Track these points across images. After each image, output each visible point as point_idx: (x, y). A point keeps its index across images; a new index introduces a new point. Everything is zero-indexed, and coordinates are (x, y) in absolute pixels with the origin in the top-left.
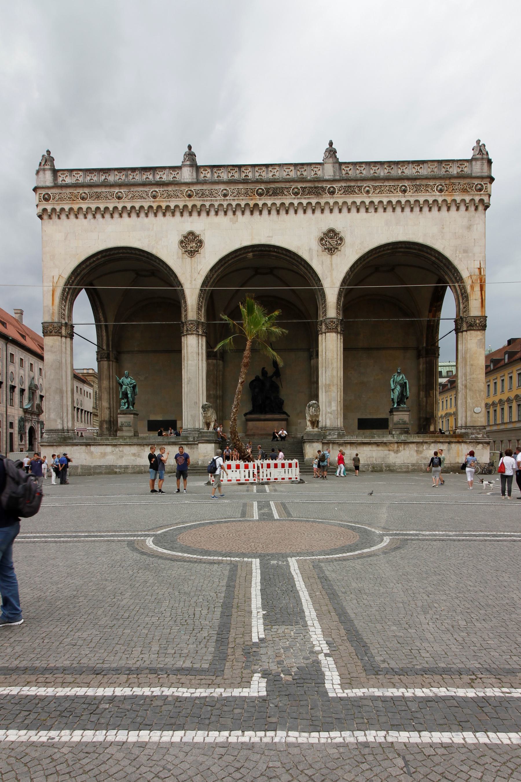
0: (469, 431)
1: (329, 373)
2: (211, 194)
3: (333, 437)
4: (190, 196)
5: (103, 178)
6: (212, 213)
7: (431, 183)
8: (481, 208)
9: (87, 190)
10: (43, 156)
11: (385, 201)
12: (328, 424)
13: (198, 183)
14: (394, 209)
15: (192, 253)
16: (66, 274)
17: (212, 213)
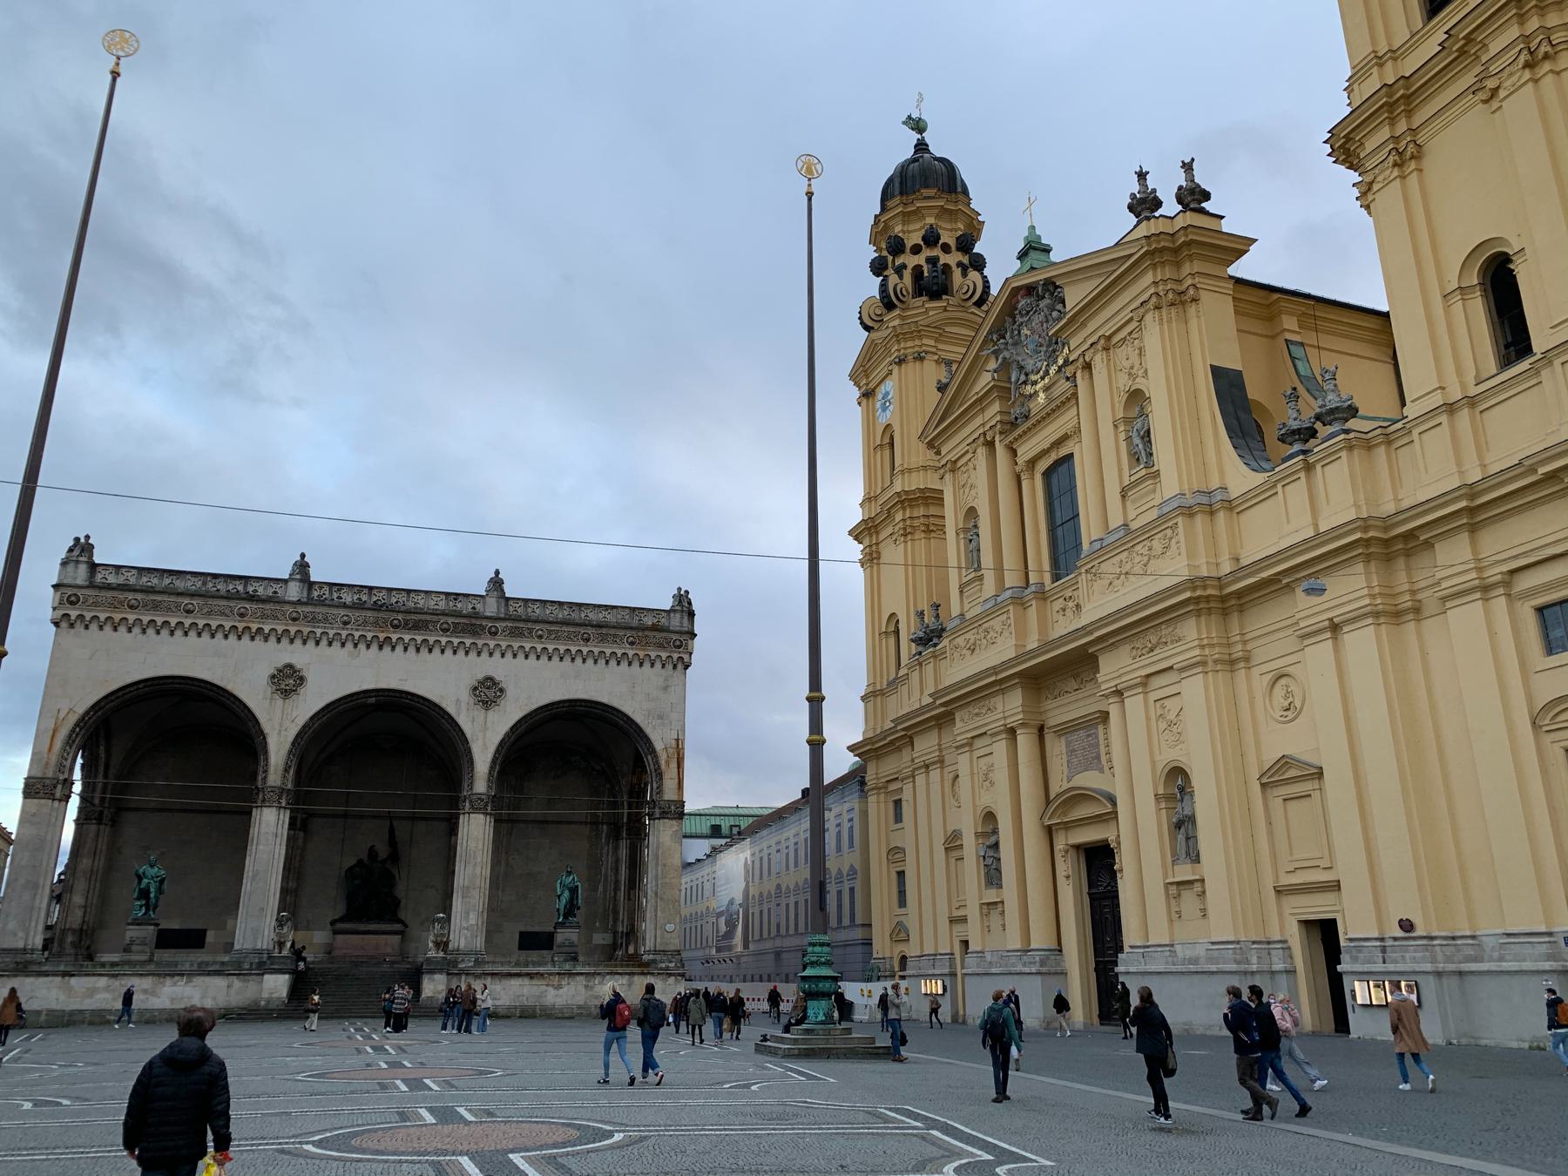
0: (658, 957)
1: (469, 870)
2: (326, 619)
3: (467, 964)
4: (294, 620)
5: (167, 581)
6: (324, 642)
7: (621, 633)
8: (680, 666)
9: (139, 596)
10: (77, 540)
11: (562, 648)
12: (462, 945)
13: (310, 602)
14: (573, 660)
15: (286, 693)
16: (81, 709)
17: (324, 642)
